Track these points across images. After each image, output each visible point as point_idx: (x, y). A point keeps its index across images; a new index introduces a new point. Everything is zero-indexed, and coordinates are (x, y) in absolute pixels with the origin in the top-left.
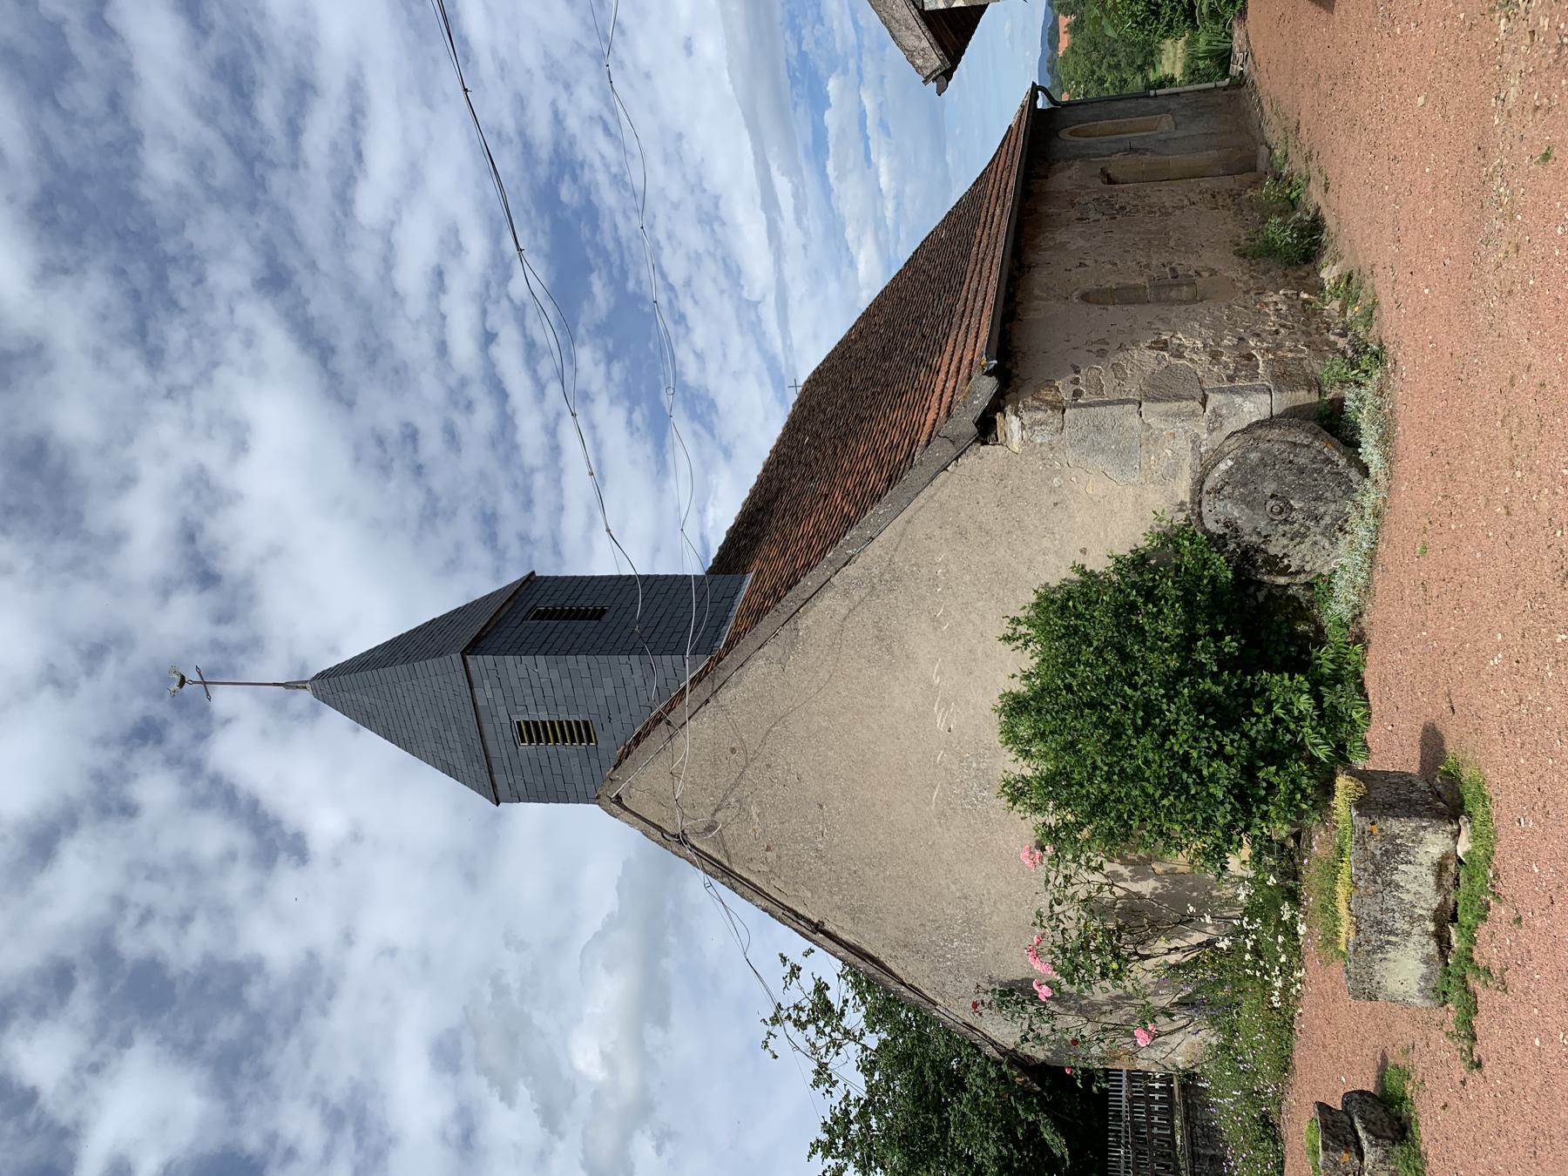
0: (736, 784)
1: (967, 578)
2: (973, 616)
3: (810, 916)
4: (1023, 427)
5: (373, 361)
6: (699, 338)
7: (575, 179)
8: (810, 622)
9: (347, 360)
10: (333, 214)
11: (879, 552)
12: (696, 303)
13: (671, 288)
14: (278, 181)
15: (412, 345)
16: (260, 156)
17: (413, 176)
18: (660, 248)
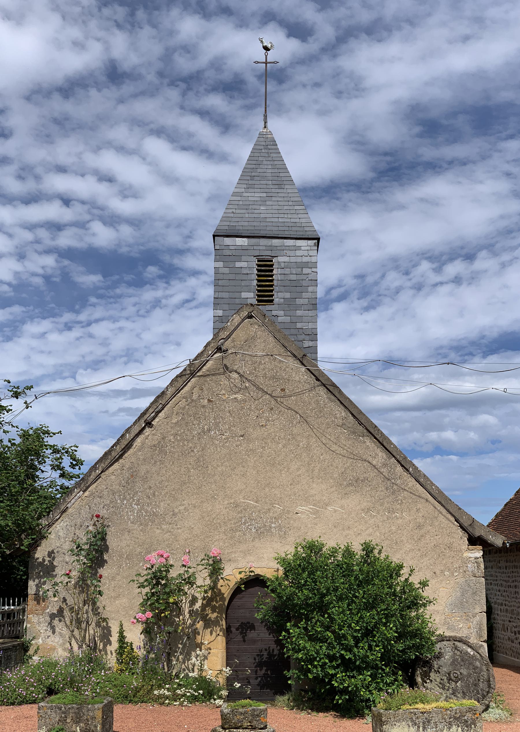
0: (259, 388)
1: (393, 528)
2: (371, 530)
3: (157, 420)
4: (476, 558)
5: (56, 121)
6: (54, 337)
7: (160, 277)
8: (368, 443)
9: (59, 106)
10: (152, 122)
11: (410, 485)
12: (78, 339)
13: (89, 324)
14: (174, 94)
15: (65, 150)
16: (189, 89)
17: (170, 179)
18: (114, 322)
